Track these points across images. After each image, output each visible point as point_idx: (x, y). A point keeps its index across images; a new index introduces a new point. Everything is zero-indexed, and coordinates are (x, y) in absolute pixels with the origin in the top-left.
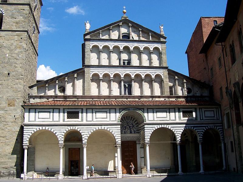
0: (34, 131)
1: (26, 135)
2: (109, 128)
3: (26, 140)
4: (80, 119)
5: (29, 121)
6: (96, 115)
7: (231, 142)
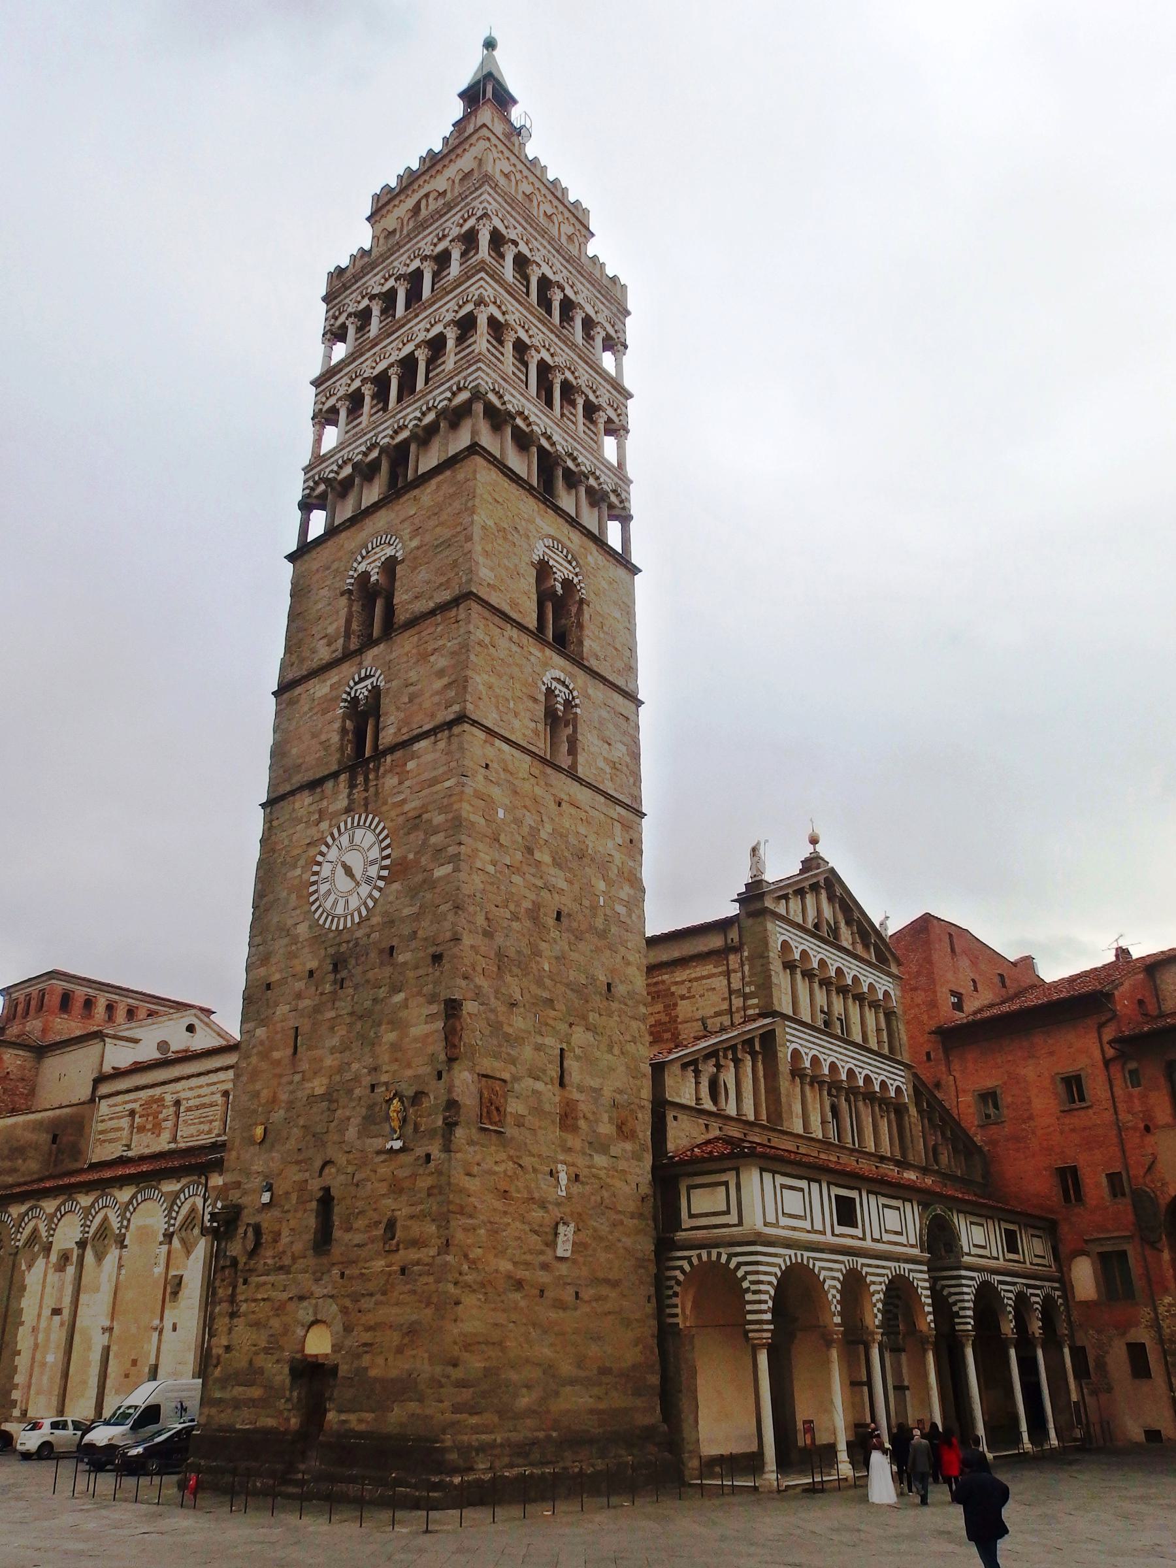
4: (858, 1232)
5: (766, 1224)
7: (1129, 1345)
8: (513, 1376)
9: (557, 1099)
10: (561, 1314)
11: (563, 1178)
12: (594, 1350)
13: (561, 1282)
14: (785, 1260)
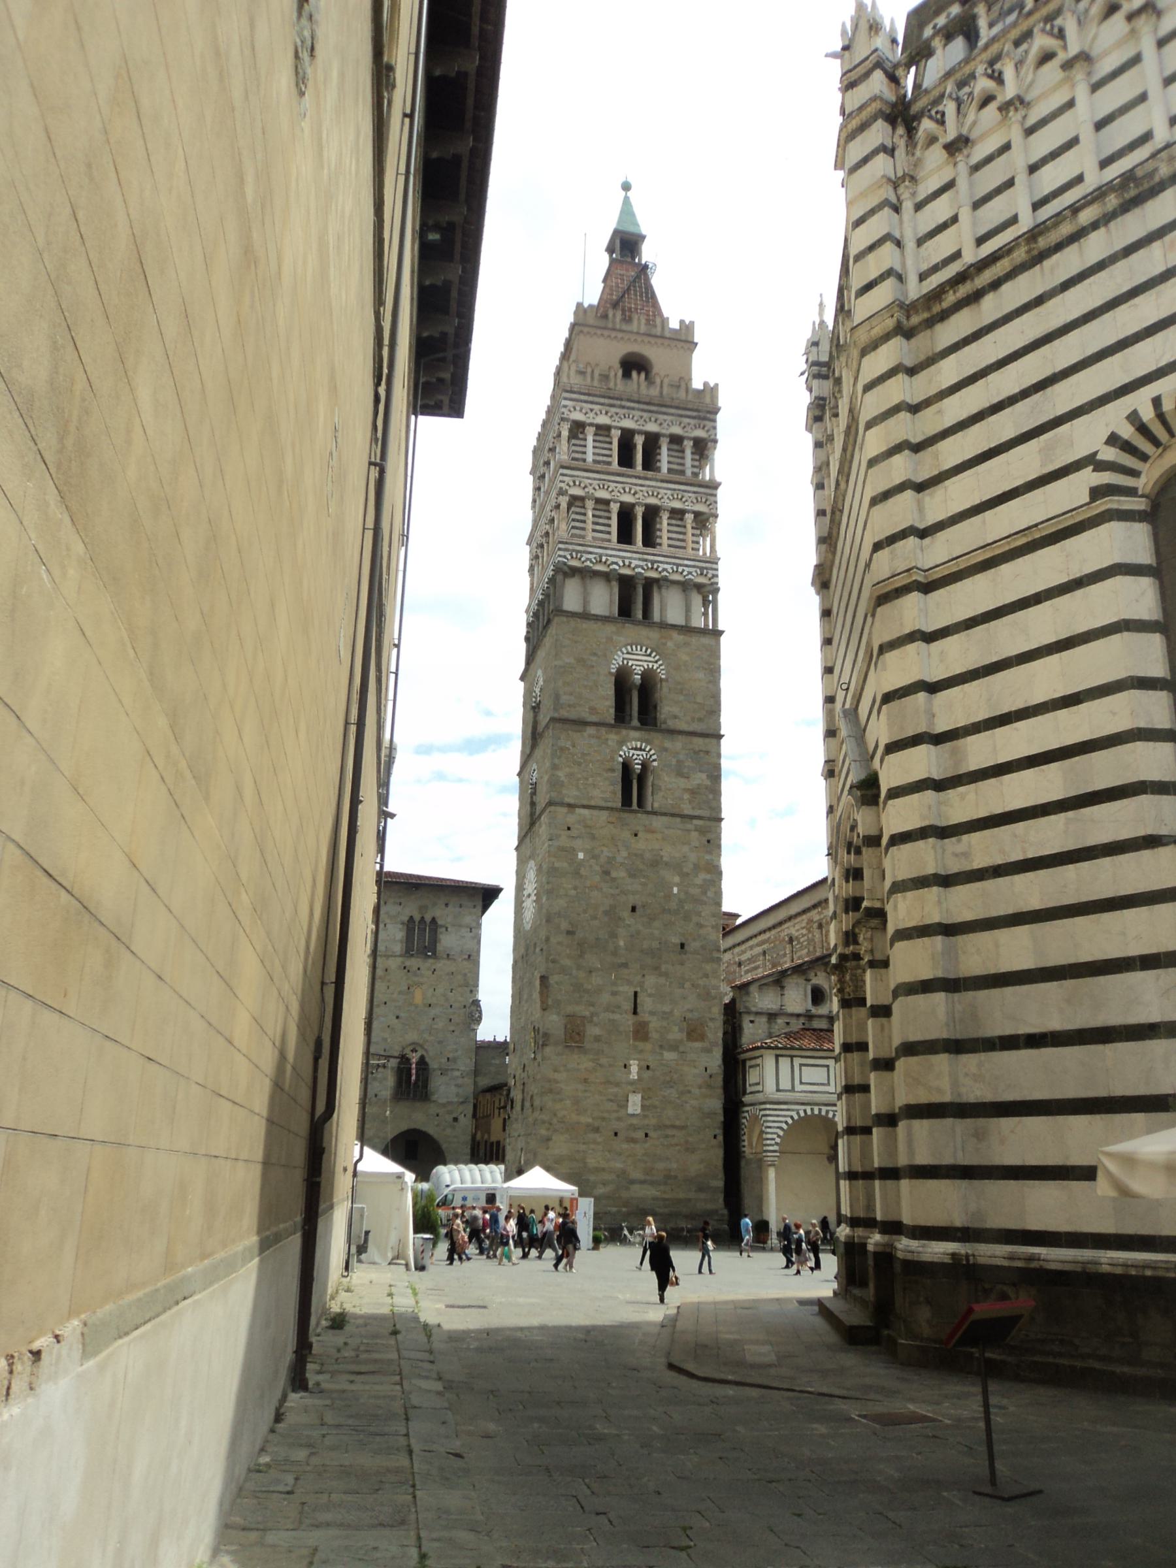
0: (792, 1117)
1: (774, 1127)
3: (773, 1142)
8: (592, 1178)
9: (630, 1023)
10: (632, 1145)
11: (634, 1069)
12: (660, 1166)
13: (635, 1128)
14: (798, 1113)
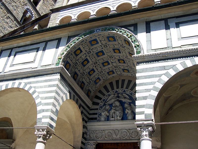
2: (30, 83)
6: (13, 60)
